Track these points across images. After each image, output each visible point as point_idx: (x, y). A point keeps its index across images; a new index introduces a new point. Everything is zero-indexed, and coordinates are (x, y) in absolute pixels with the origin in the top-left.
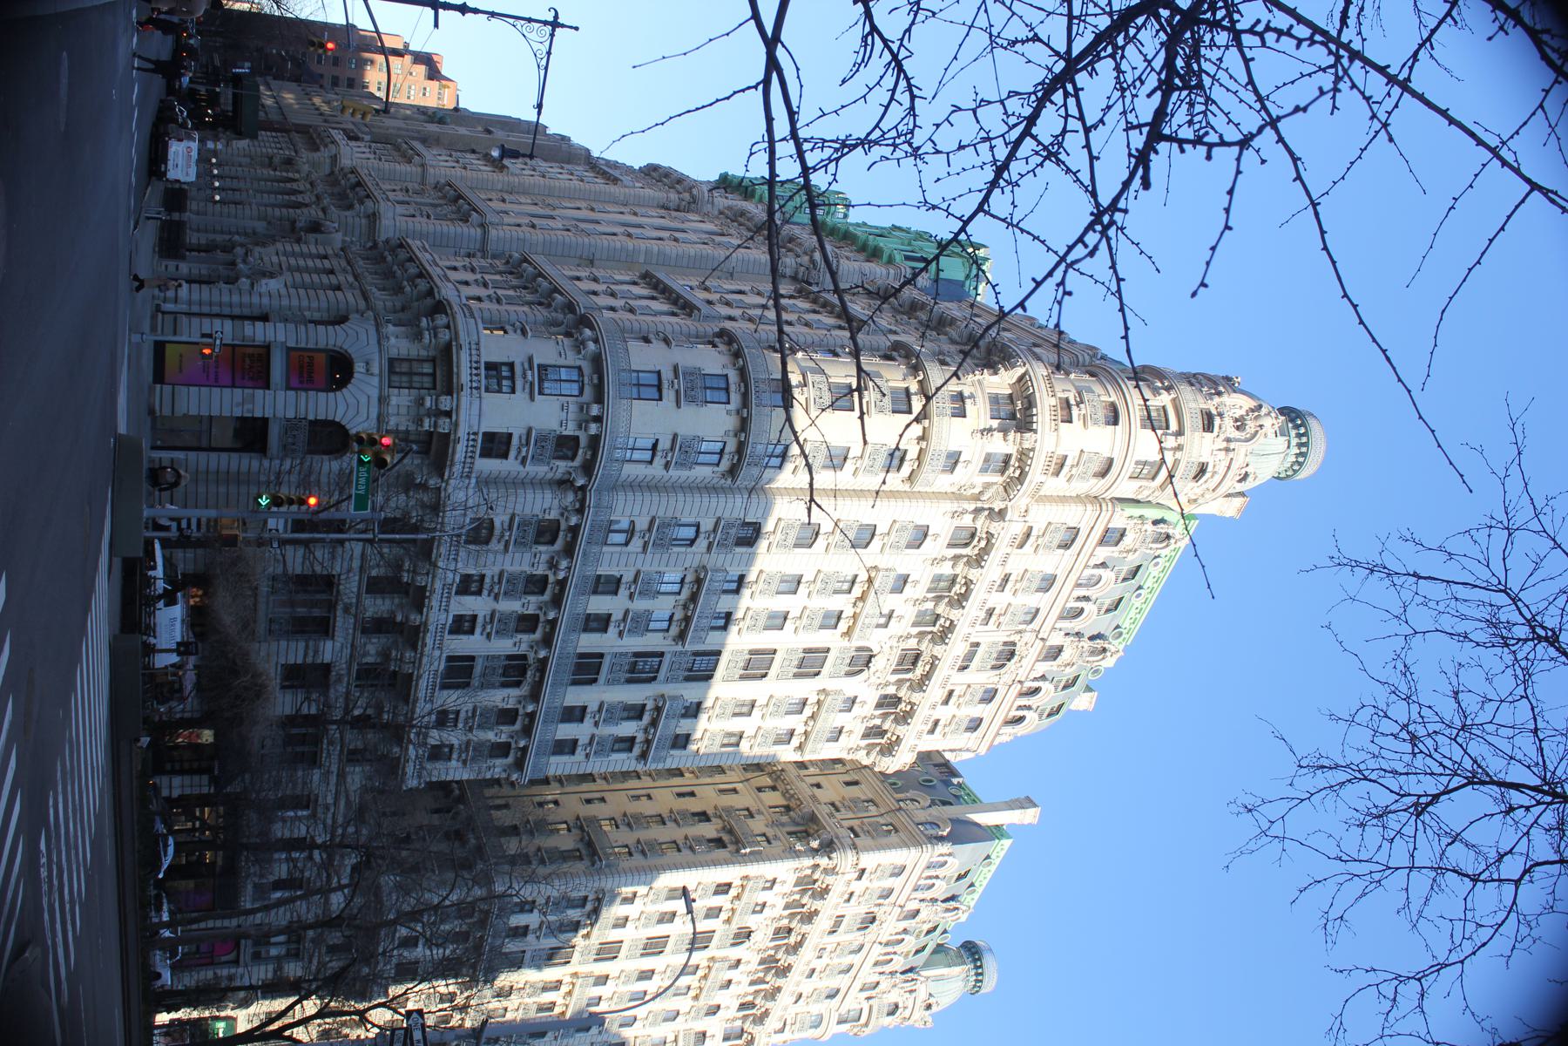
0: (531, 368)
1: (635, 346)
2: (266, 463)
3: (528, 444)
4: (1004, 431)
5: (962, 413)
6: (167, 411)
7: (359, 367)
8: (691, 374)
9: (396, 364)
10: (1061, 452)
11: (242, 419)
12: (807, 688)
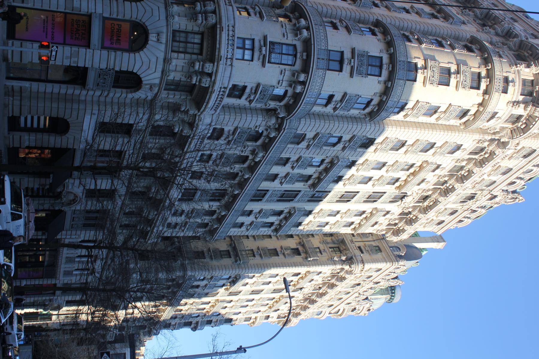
0: (265, 45)
1: (330, 30)
2: (84, 92)
3: (256, 93)
4: (526, 103)
5: (505, 91)
6: (17, 59)
7: (152, 37)
8: (362, 56)
9: (178, 34)
11: (70, 67)
12: (368, 207)
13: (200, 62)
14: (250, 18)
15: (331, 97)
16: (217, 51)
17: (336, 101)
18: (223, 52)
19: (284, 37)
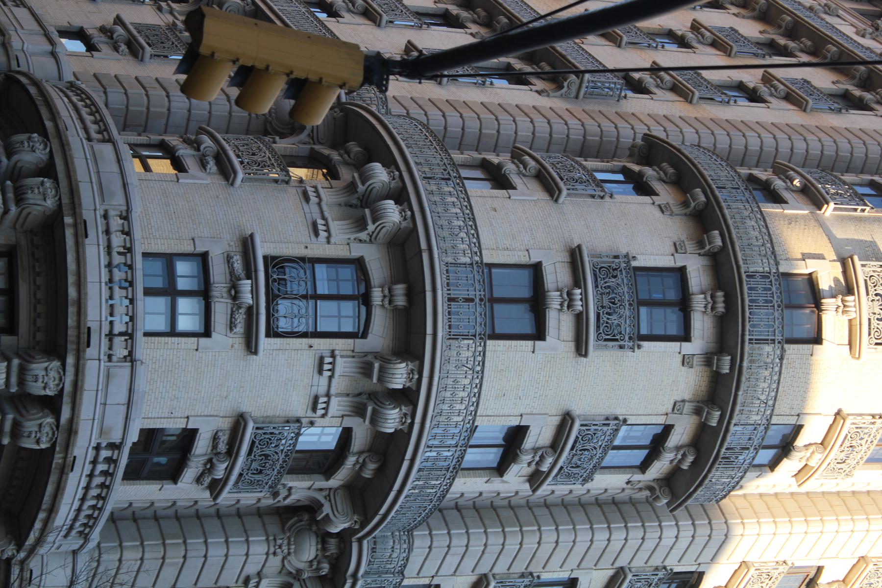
0: (250, 272)
3: (232, 452)
13: (9, 360)
14: (184, 180)
15: (515, 437)
16: (72, 310)
17: (535, 450)
18: (95, 313)
19: (317, 234)
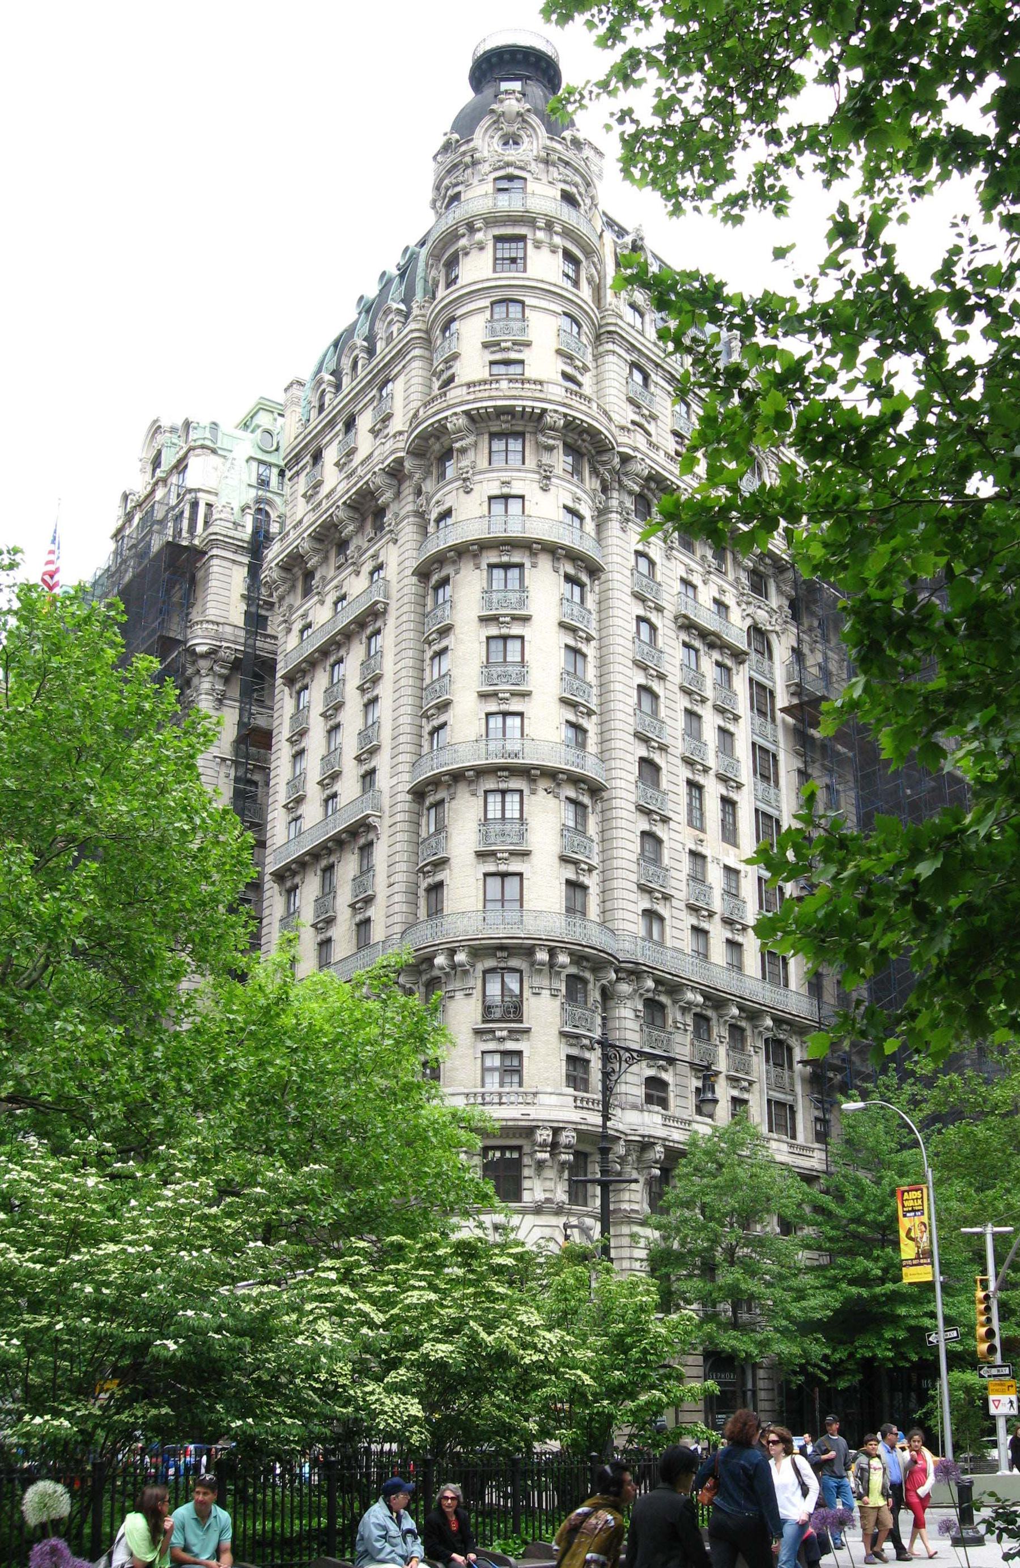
0: (492, 1031)
3: (577, 1037)
10: (559, 378)
